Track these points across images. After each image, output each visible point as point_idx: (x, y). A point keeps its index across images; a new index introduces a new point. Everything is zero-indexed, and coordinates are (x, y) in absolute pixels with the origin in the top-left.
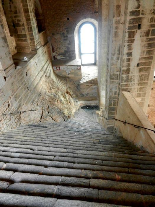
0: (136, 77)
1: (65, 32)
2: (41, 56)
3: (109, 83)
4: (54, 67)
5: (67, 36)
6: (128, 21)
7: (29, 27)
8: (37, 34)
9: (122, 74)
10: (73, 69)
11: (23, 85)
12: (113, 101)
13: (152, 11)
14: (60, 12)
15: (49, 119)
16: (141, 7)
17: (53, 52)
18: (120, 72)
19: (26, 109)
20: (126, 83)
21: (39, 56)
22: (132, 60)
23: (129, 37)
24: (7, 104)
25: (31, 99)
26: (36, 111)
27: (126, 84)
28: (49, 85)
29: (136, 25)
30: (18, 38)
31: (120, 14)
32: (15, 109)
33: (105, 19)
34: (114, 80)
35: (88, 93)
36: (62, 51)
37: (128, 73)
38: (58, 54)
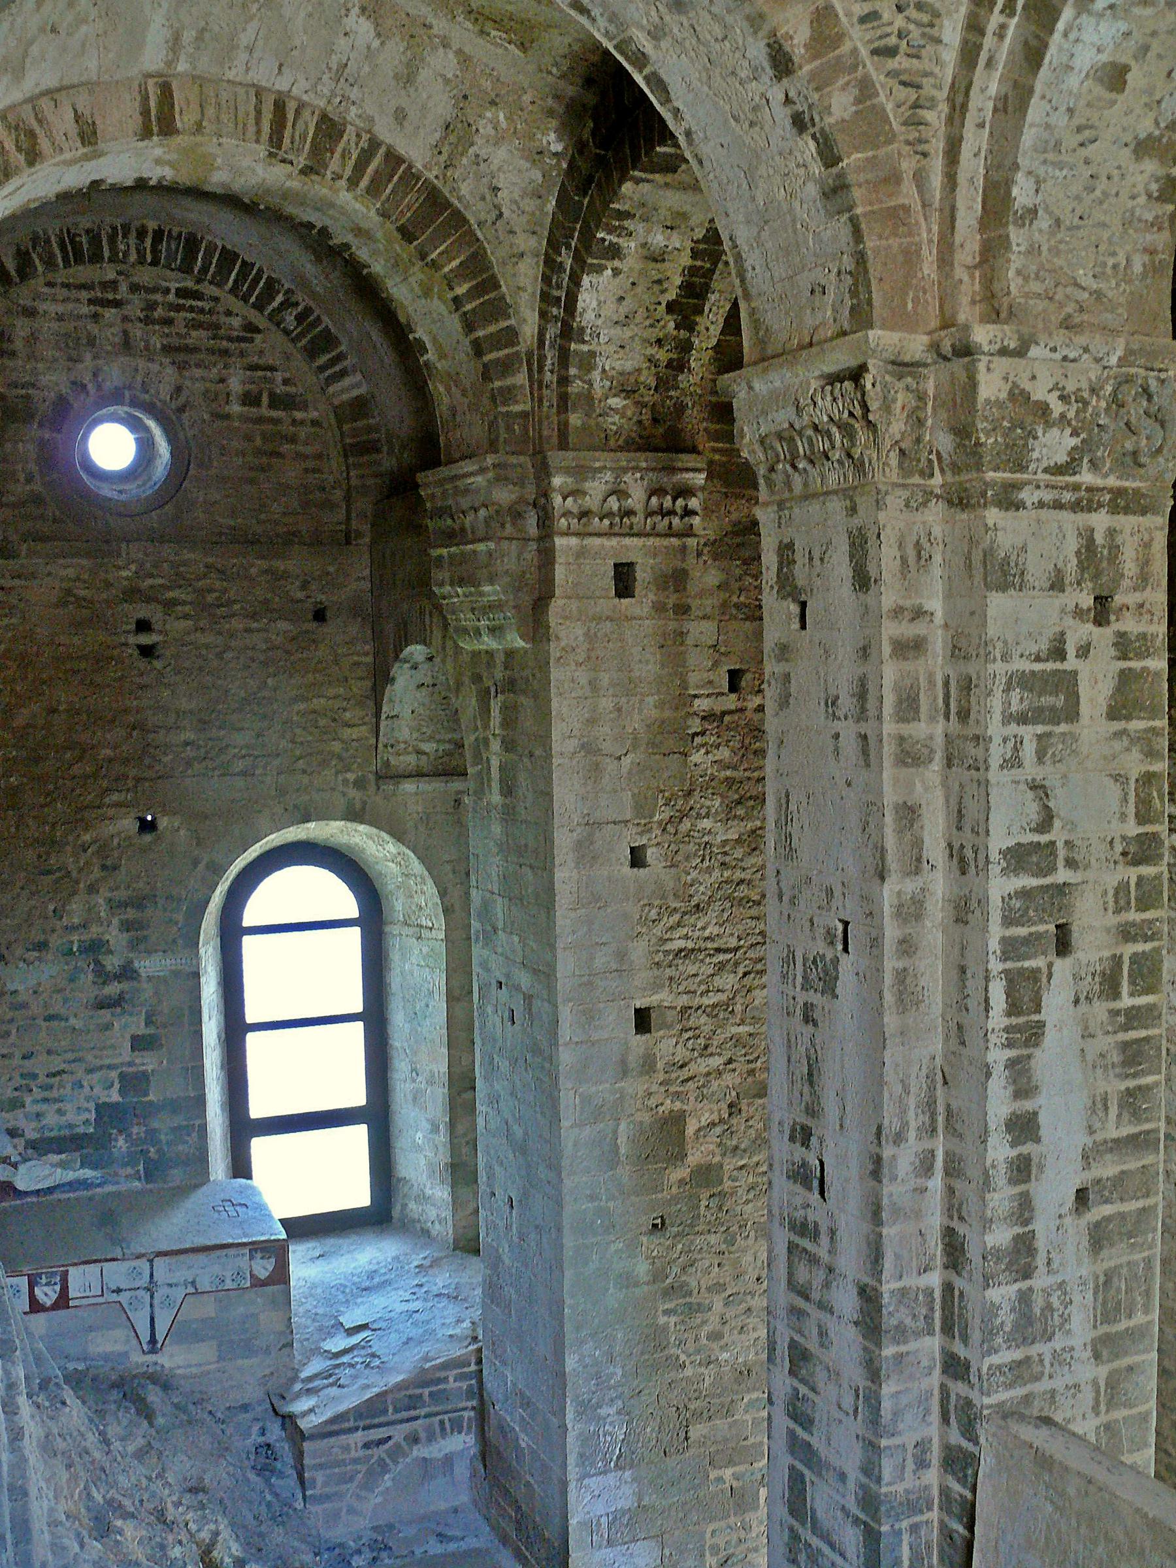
0: (1077, 1298)
1: (115, 937)
5: (127, 973)
10: (205, 1284)
12: (906, 1537)
13: (1119, 848)
14: (76, 770)
16: (1057, 823)
20: (1018, 1355)
22: (1041, 1168)
23: (1013, 1009)
27: (1019, 1363)
28: (74, 1478)
29: (1041, 928)
33: (579, 845)
34: (905, 1342)
35: (375, 1529)
36: (68, 1106)
37: (1027, 1273)
38: (32, 1145)
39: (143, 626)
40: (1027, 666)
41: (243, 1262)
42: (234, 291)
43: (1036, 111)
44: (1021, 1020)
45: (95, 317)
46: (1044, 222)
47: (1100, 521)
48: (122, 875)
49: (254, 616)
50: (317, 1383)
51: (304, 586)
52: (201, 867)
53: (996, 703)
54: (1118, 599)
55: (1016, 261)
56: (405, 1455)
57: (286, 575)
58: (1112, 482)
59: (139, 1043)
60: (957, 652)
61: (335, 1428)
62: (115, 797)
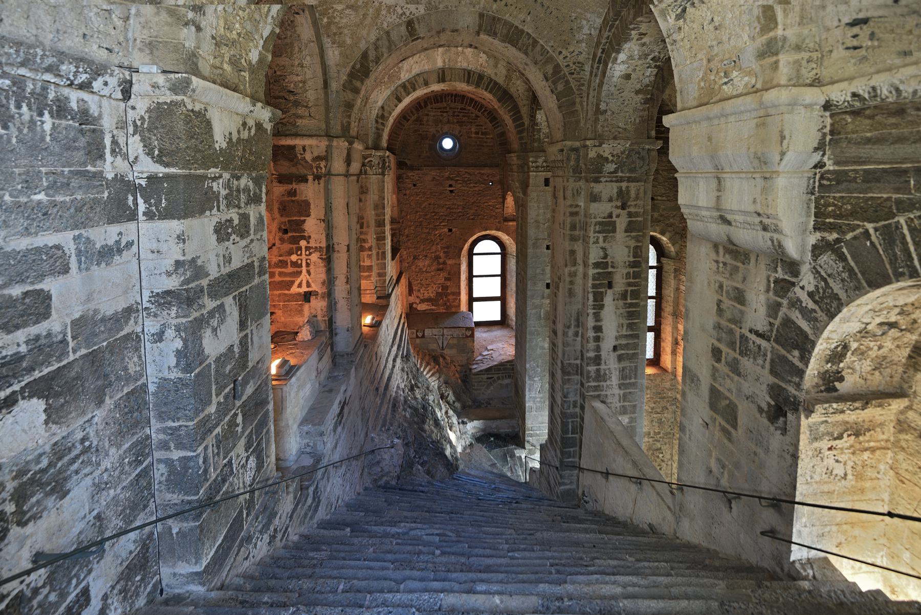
3: (560, 381)
18: (582, 359)
26: (393, 450)
40: (601, 220)
43: (605, 87)
46: (609, 113)
47: (624, 185)
53: (592, 228)
54: (629, 203)
55: (601, 123)
58: (627, 175)
60: (585, 216)
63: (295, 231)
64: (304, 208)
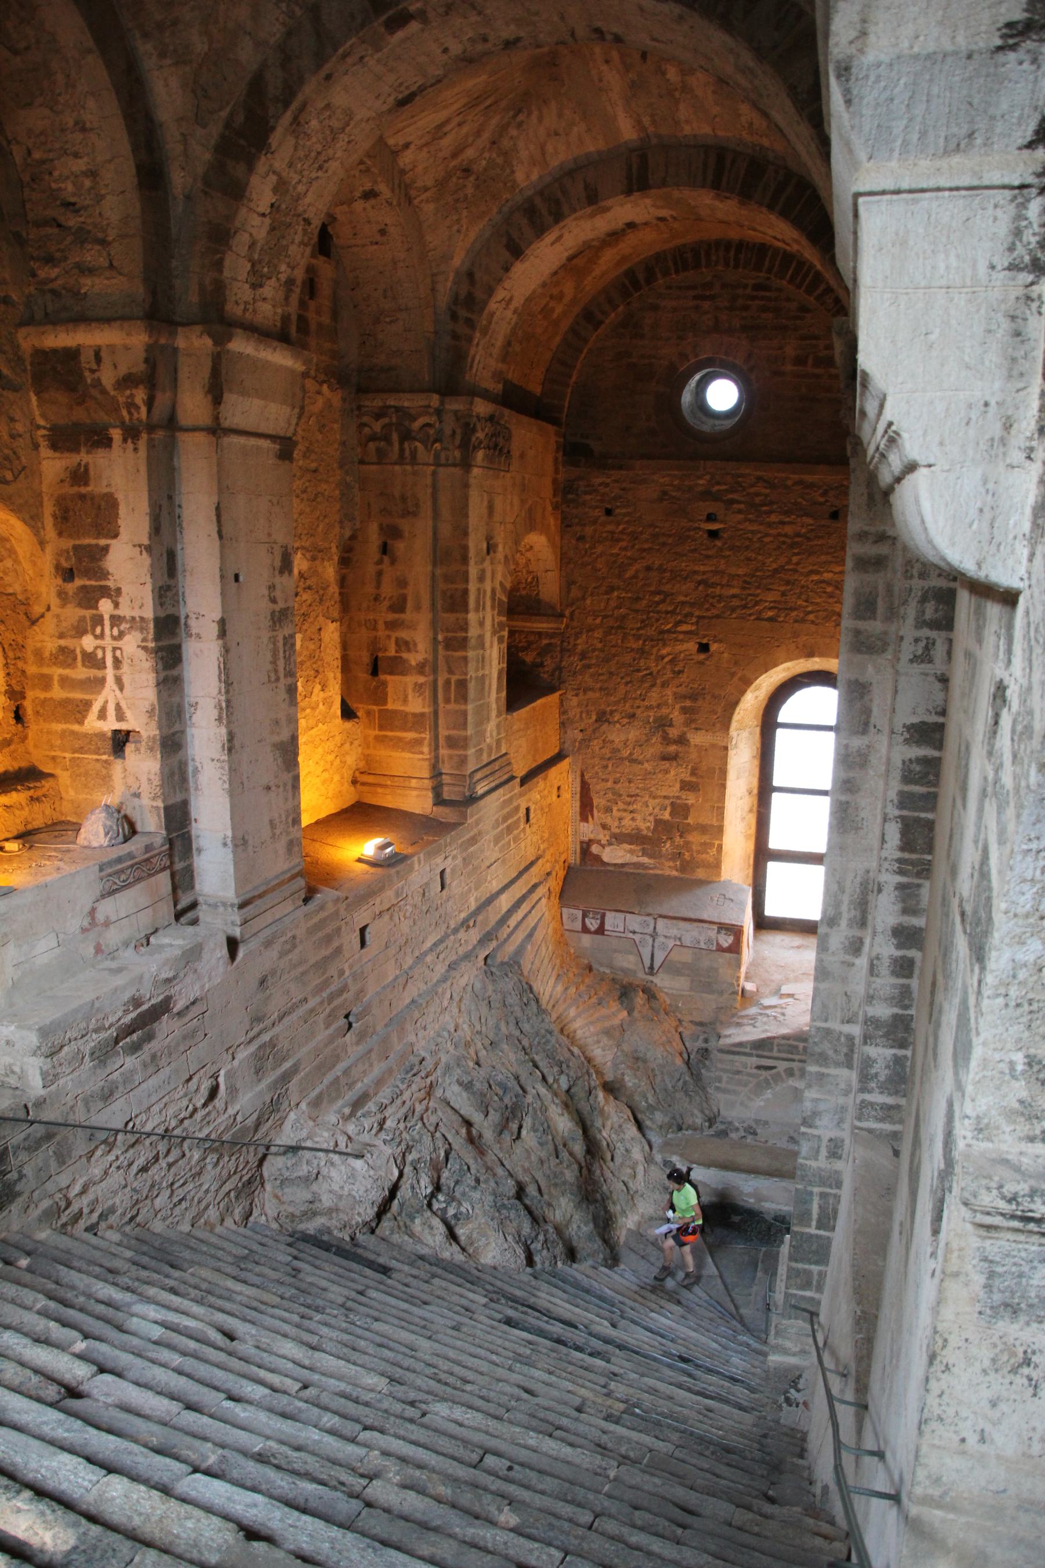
1: (676, 716)
2: (489, 837)
4: (565, 910)
5: (682, 740)
6: (899, 764)
7: (454, 679)
8: (494, 713)
9: (865, 1043)
11: (324, 995)
14: (662, 607)
15: (431, 1228)
17: (584, 818)
19: (304, 1134)
20: (890, 1100)
21: (473, 840)
23: (907, 845)
24: (206, 1086)
25: (350, 1086)
26: (358, 1164)
27: (890, 1108)
30: (381, 728)
31: (866, 724)
32: (239, 1118)
34: (827, 1066)
35: (757, 1121)
36: (638, 817)
39: (711, 518)
41: (712, 932)
42: (791, 281)
44: (914, 856)
45: (697, 308)
48: (683, 678)
49: (787, 513)
50: (745, 1021)
51: (825, 494)
52: (736, 679)
56: (783, 1080)
57: (811, 486)
59: (686, 786)
61: (737, 1050)
62: (684, 628)
63: (88, 573)
64: (102, 516)
